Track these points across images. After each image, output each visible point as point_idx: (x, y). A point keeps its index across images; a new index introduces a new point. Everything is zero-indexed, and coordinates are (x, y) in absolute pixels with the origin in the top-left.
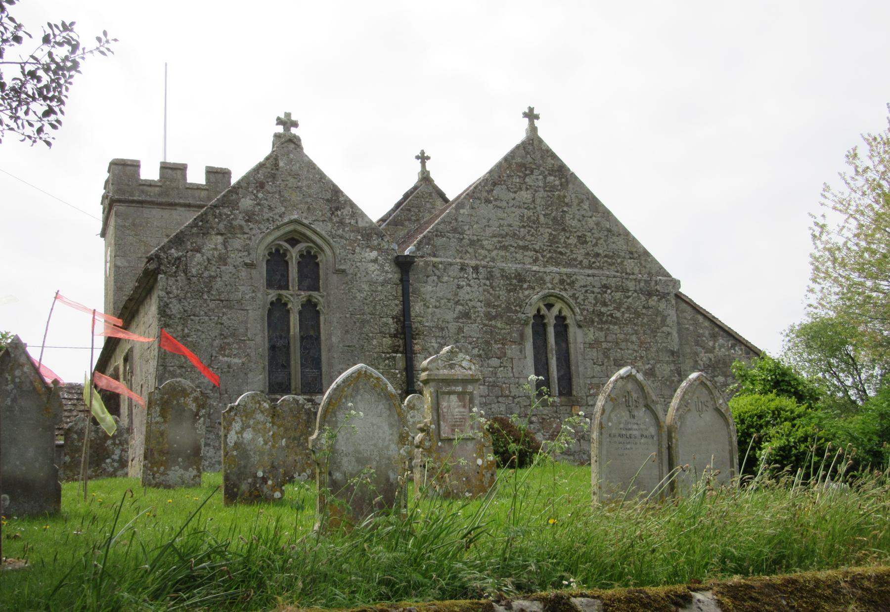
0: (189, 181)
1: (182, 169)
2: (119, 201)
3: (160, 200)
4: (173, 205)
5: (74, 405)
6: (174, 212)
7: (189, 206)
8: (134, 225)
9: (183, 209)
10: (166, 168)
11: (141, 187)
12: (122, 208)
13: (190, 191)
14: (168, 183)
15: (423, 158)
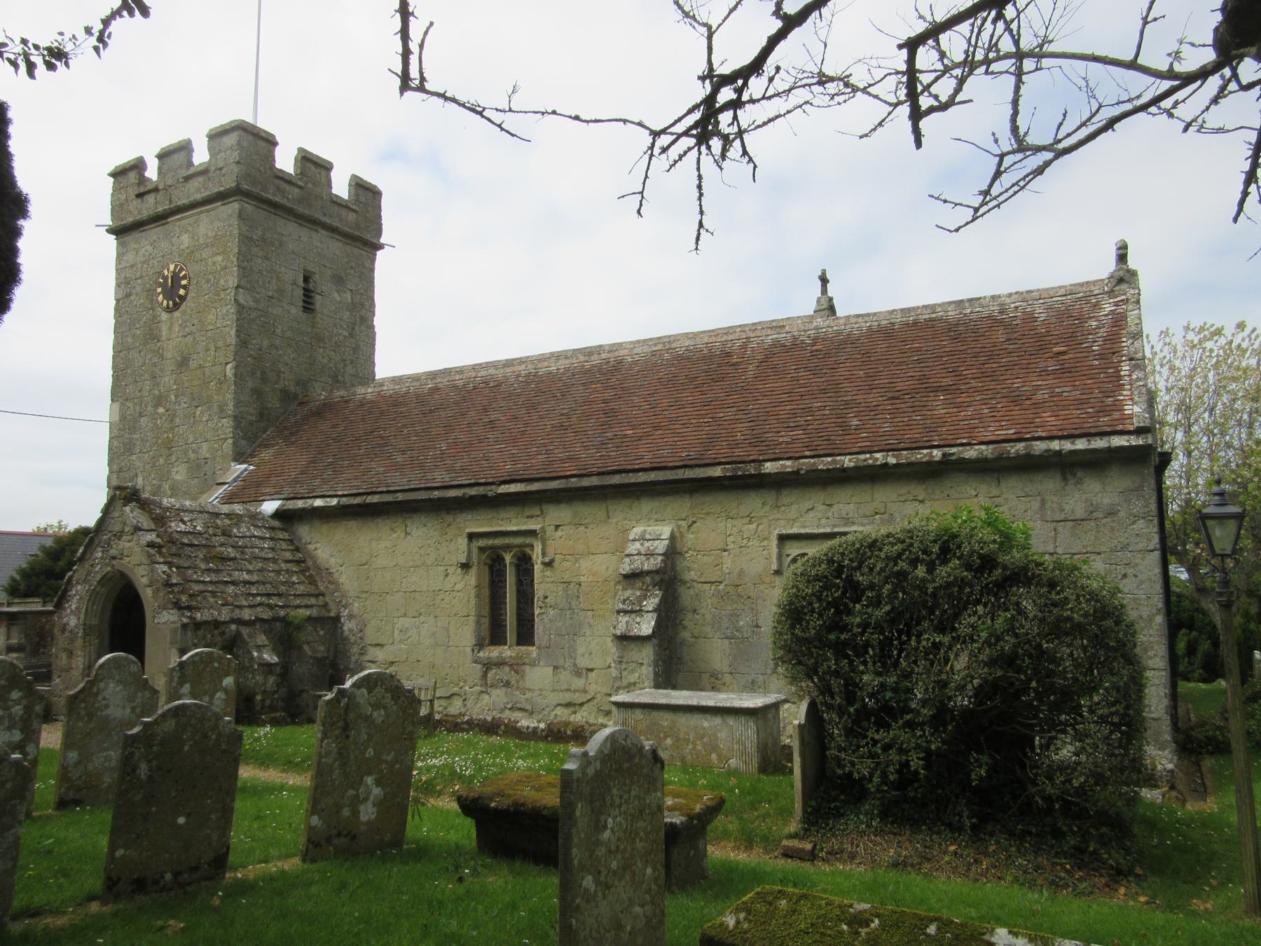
1: (326, 167)
2: (248, 195)
3: (301, 209)
4: (313, 223)
5: (273, 549)
6: (314, 234)
7: (333, 230)
8: (264, 240)
9: (324, 232)
10: (307, 160)
11: (277, 181)
12: (249, 208)
13: (336, 208)
14: (310, 185)
15: (824, 280)
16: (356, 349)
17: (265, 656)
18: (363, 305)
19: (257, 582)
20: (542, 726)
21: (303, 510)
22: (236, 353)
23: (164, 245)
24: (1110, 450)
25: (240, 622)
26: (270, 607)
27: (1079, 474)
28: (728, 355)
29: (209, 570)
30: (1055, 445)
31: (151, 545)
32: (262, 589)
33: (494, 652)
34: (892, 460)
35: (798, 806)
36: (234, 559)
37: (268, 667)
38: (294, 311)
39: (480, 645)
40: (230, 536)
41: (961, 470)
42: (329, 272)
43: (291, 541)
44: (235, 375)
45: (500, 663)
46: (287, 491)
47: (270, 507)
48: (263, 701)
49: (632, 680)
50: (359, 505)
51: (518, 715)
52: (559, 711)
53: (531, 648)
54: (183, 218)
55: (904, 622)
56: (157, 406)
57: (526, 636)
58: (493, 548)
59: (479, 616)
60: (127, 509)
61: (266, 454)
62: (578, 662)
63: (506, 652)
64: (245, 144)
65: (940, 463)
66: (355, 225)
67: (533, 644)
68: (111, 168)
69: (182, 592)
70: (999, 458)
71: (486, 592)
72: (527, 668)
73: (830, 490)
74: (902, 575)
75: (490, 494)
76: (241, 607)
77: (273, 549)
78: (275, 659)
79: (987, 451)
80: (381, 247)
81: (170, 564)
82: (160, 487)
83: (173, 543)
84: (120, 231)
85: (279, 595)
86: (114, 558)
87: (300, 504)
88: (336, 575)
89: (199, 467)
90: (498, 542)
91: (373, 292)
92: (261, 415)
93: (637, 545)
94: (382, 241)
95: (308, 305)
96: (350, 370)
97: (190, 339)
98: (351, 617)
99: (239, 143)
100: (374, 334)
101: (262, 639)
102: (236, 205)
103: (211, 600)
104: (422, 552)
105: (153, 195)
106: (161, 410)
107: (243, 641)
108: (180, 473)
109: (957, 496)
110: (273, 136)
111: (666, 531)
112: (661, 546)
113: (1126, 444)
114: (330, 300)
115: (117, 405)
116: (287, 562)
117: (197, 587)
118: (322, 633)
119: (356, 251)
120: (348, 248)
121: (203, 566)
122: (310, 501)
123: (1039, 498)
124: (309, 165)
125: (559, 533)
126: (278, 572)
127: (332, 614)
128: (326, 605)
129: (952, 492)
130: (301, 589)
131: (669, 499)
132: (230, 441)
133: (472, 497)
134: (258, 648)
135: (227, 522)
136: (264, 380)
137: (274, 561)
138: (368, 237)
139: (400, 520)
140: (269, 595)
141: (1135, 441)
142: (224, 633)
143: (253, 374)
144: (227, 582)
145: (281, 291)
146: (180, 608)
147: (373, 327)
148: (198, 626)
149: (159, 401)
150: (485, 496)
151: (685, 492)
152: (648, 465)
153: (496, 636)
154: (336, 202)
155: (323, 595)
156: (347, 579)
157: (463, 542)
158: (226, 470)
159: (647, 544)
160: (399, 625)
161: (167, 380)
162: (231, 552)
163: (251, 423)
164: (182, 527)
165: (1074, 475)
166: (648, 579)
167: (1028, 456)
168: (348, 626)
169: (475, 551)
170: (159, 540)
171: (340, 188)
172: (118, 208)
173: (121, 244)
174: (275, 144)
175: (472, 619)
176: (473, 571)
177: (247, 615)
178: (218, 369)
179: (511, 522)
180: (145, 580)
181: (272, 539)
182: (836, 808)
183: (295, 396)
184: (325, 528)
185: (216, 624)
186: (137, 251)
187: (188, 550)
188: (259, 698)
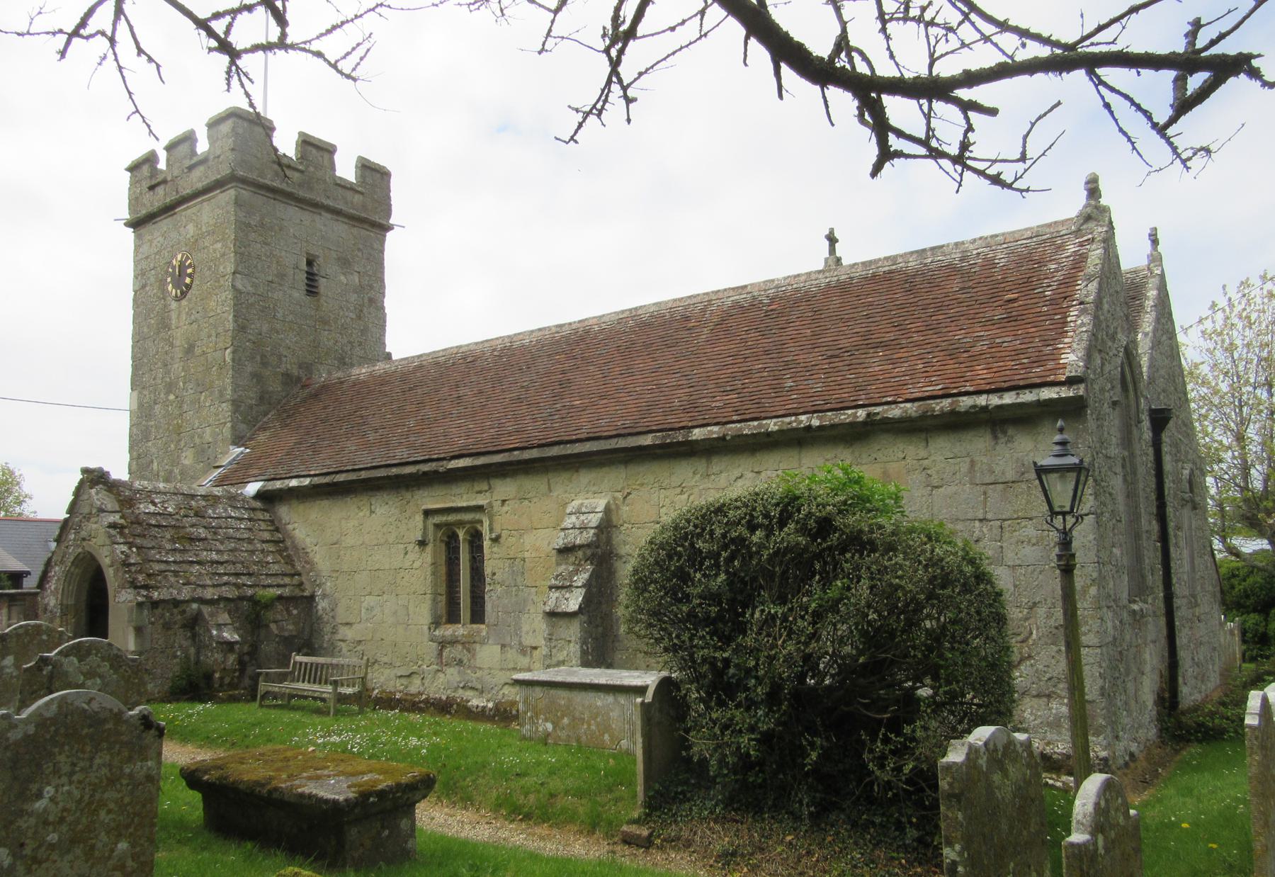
0: (338, 174)
1: (329, 150)
2: (244, 181)
3: (301, 193)
4: (315, 206)
5: (250, 529)
6: (317, 217)
7: (337, 212)
9: (329, 216)
10: (307, 143)
12: (246, 194)
14: (312, 169)
15: (832, 239)
16: (364, 331)
17: (225, 634)
18: (371, 287)
19: (226, 562)
20: (490, 705)
21: (281, 490)
22: (234, 338)
23: (174, 235)
24: (1039, 403)
25: (202, 601)
26: (237, 586)
27: (1010, 432)
28: (687, 319)
29: (175, 550)
30: (982, 400)
31: (113, 526)
32: (231, 569)
33: (448, 631)
34: (816, 422)
35: (640, 789)
36: (206, 539)
37: (230, 646)
38: (296, 295)
39: (436, 623)
40: (203, 517)
41: (887, 431)
42: (334, 255)
43: (272, 522)
44: (233, 360)
45: (453, 642)
46: (271, 472)
47: (252, 488)
48: (221, 678)
49: (561, 658)
50: (327, 484)
51: (469, 694)
52: (507, 690)
53: (483, 626)
54: (188, 208)
55: (742, 593)
56: (168, 393)
57: (478, 615)
58: (447, 525)
59: (435, 594)
60: (93, 491)
61: (262, 437)
62: (523, 640)
63: (460, 630)
64: (240, 131)
65: (864, 423)
66: (363, 208)
67: (483, 622)
68: (128, 163)
69: (140, 572)
70: (923, 417)
71: (443, 570)
72: (478, 646)
73: (758, 456)
74: (741, 540)
75: (441, 469)
76: (204, 586)
77: (250, 529)
78: (237, 637)
79: (911, 409)
80: (389, 228)
81: (131, 545)
82: (171, 472)
83: (140, 524)
84: (136, 224)
85: (250, 575)
86: (84, 539)
87: (278, 485)
88: (311, 555)
89: (203, 451)
90: (452, 518)
91: (383, 273)
92: (261, 398)
93: (573, 518)
94: (391, 221)
95: (312, 288)
96: (358, 351)
97: (195, 326)
98: (324, 596)
99: (233, 129)
100: (384, 315)
101: (224, 617)
102: (232, 192)
103: (172, 579)
104: (385, 530)
105: (162, 186)
106: (172, 397)
107: (204, 619)
108: (188, 458)
109: (885, 459)
110: (271, 122)
111: (601, 504)
112: (594, 519)
113: (1055, 396)
114: (334, 281)
115: (136, 393)
116: (263, 542)
117: (157, 567)
118: (295, 612)
119: (364, 232)
120: (355, 231)
121: (168, 546)
122: (286, 481)
123: (968, 460)
124: (310, 148)
125: (506, 508)
126: (253, 552)
127: (307, 594)
128: (301, 584)
129: (879, 455)
130: (275, 568)
131: (606, 469)
132: (229, 425)
133: (425, 473)
134: (219, 627)
135: (204, 503)
136: (264, 364)
137: (250, 541)
138: (376, 218)
139: (365, 499)
140: (237, 575)
141: (1065, 392)
142: (184, 612)
143: (252, 358)
144: (192, 562)
145: (282, 276)
146: (136, 587)
147: (383, 308)
148: (155, 604)
149: (170, 388)
150: (436, 472)
151: (620, 462)
152: (585, 435)
153: (453, 617)
154: (343, 185)
155: (299, 575)
156: (321, 559)
157: (419, 518)
158: (225, 453)
159: (582, 517)
160: (365, 605)
161: (177, 367)
162: (202, 532)
163: (251, 407)
164: (152, 508)
165: (1005, 433)
166: (580, 554)
167: (953, 413)
168: (322, 605)
169: (431, 528)
170: (122, 521)
171: (346, 170)
172: (134, 202)
173: (138, 237)
174: (273, 129)
175: (428, 596)
176: (429, 549)
177: (209, 594)
178: (219, 353)
179: (462, 497)
180: (107, 561)
181: (250, 520)
182: (683, 792)
183: (299, 379)
184: (301, 507)
185: (176, 603)
186: (151, 241)
187: (154, 531)
188: (217, 675)
